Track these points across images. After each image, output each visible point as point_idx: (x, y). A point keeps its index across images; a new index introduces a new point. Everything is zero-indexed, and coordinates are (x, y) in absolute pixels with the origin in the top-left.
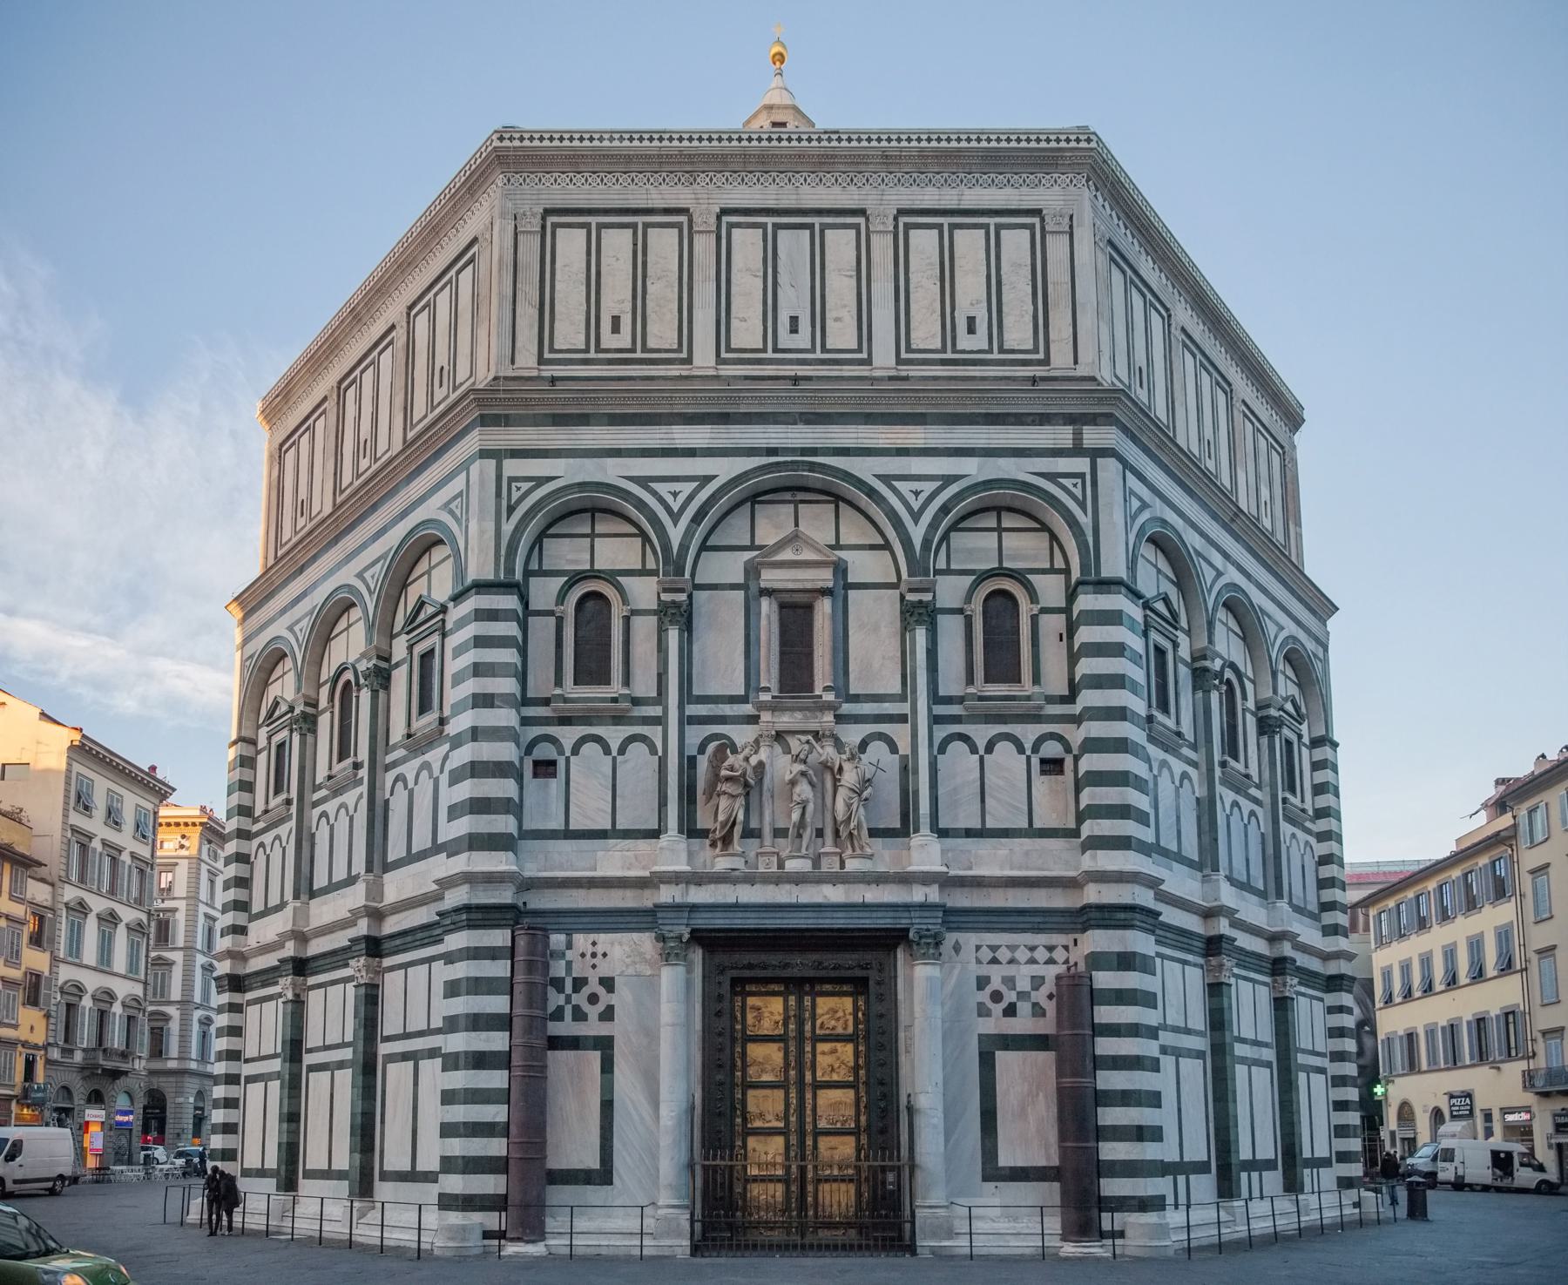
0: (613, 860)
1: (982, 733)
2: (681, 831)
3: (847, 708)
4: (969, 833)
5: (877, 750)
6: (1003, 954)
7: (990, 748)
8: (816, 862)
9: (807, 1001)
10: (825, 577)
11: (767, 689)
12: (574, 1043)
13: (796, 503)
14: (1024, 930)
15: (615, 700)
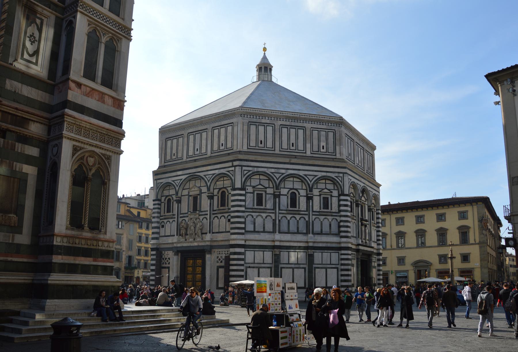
0: (170, 240)
1: (219, 216)
2: (177, 235)
3: (201, 213)
4: (217, 233)
5: (205, 219)
6: (221, 253)
7: (220, 218)
8: (194, 240)
9: (195, 261)
10: (198, 192)
11: (190, 212)
12: (165, 268)
13: (195, 180)
14: (224, 248)
15: (171, 215)
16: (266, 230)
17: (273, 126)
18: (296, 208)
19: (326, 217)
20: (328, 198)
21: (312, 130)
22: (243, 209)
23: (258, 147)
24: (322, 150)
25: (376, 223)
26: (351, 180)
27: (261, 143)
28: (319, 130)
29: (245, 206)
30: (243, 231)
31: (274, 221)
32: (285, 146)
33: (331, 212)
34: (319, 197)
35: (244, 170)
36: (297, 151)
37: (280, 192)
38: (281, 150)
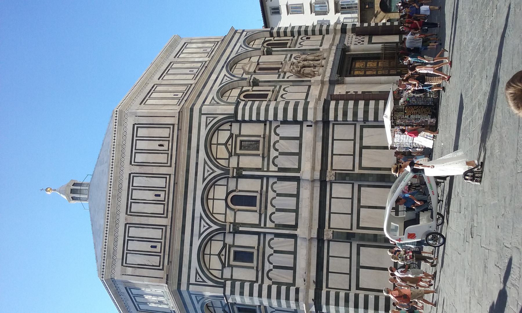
16: (293, 250)
17: (129, 227)
18: (256, 196)
19: (272, 144)
20: (241, 141)
21: (134, 162)
22: (256, 286)
23: (161, 252)
24: (165, 148)
25: (291, 38)
26: (213, 98)
27: (155, 247)
28: (134, 151)
29: (252, 283)
30: (293, 289)
31: (277, 235)
32: (159, 209)
33: (264, 138)
34: (241, 157)
35: (196, 281)
36: (167, 189)
37: (231, 223)
38: (165, 215)
